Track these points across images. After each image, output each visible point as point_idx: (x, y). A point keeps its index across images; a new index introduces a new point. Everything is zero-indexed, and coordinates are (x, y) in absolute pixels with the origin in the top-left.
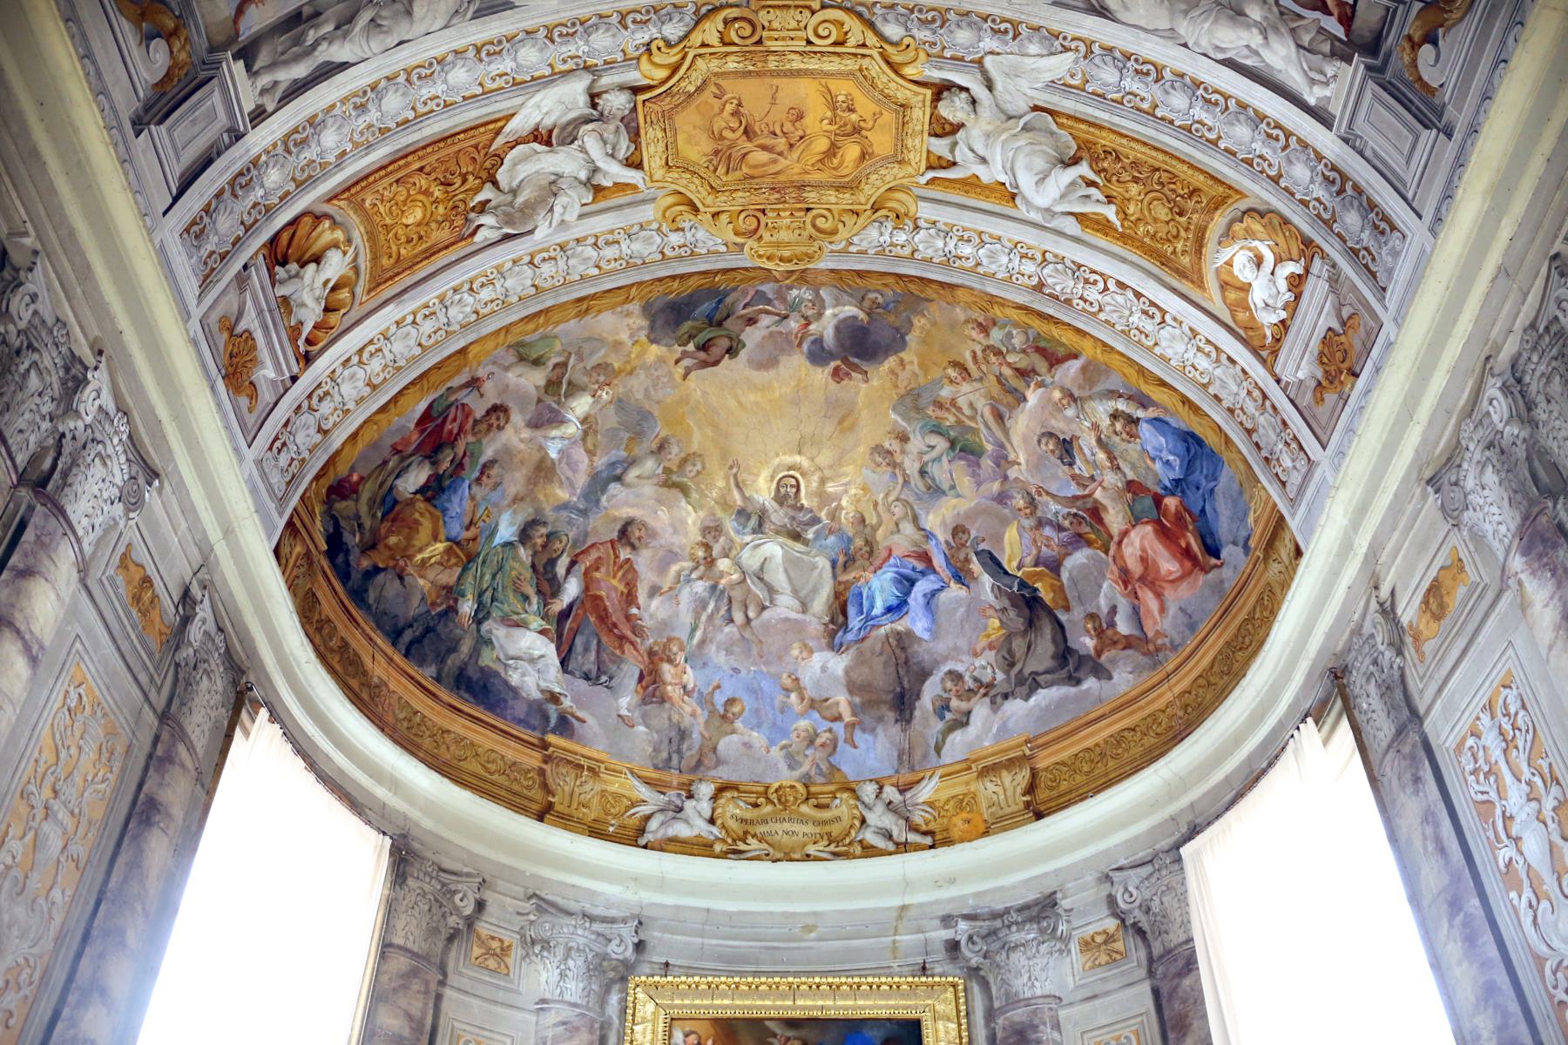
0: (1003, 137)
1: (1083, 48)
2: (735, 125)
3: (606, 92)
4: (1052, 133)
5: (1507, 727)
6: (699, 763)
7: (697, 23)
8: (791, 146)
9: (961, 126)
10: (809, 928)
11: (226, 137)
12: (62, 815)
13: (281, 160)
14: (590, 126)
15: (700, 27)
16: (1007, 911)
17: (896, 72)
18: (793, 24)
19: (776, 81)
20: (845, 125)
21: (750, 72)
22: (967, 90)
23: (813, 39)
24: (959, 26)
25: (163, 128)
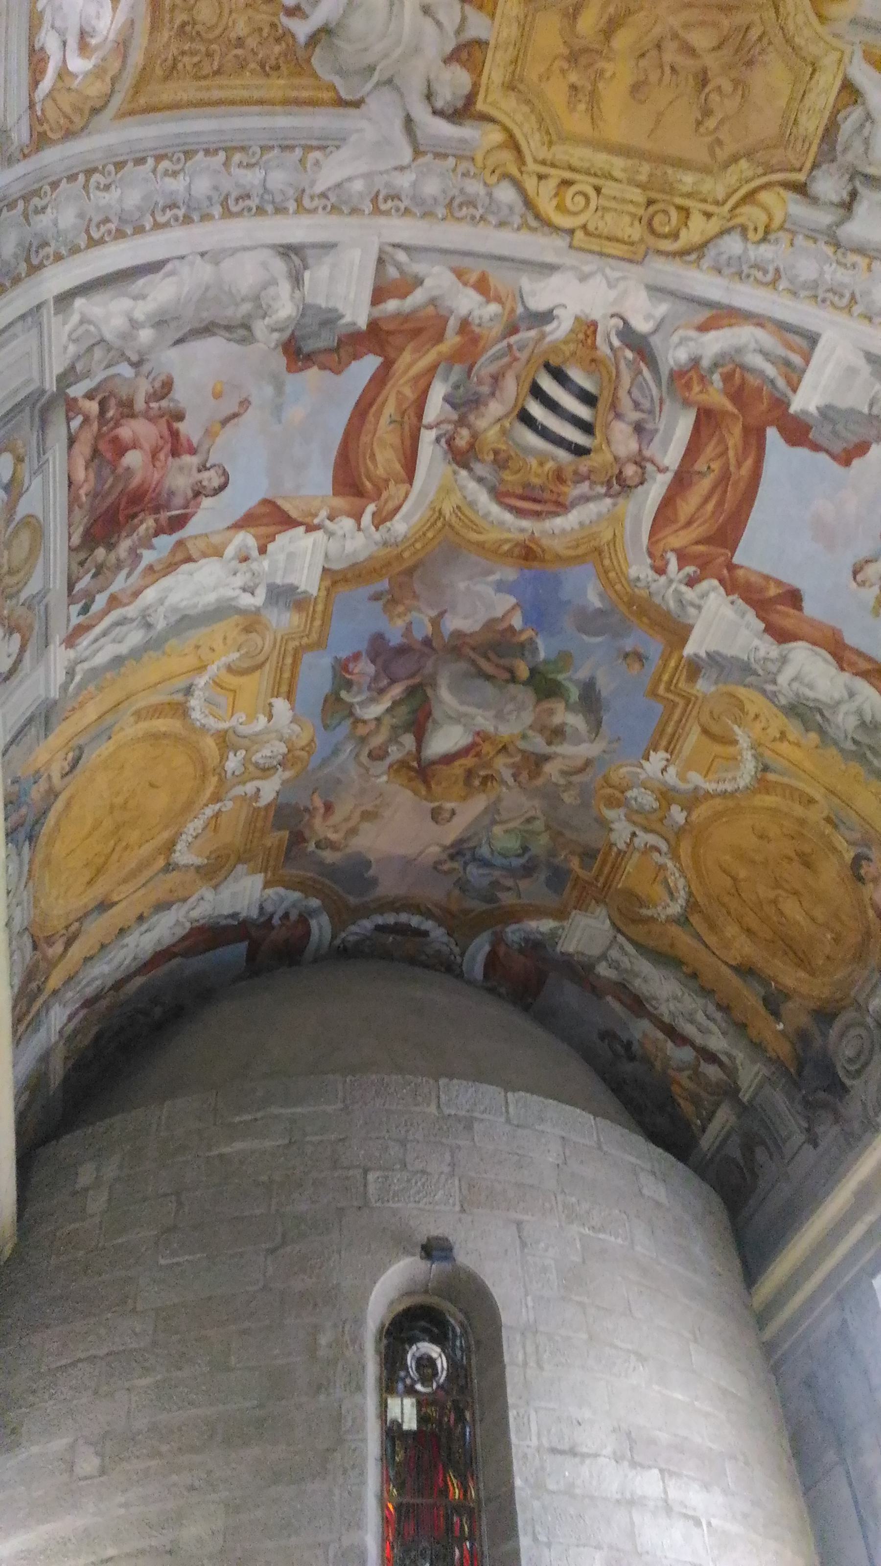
0: (399, 51)
1: (306, 202)
2: (715, 97)
3: (832, 204)
7: (705, 244)
8: (659, 47)
15: (704, 239)
17: (511, 136)
18: (609, 217)
19: (648, 145)
21: (673, 166)
22: (435, 112)
23: (592, 194)
24: (435, 200)
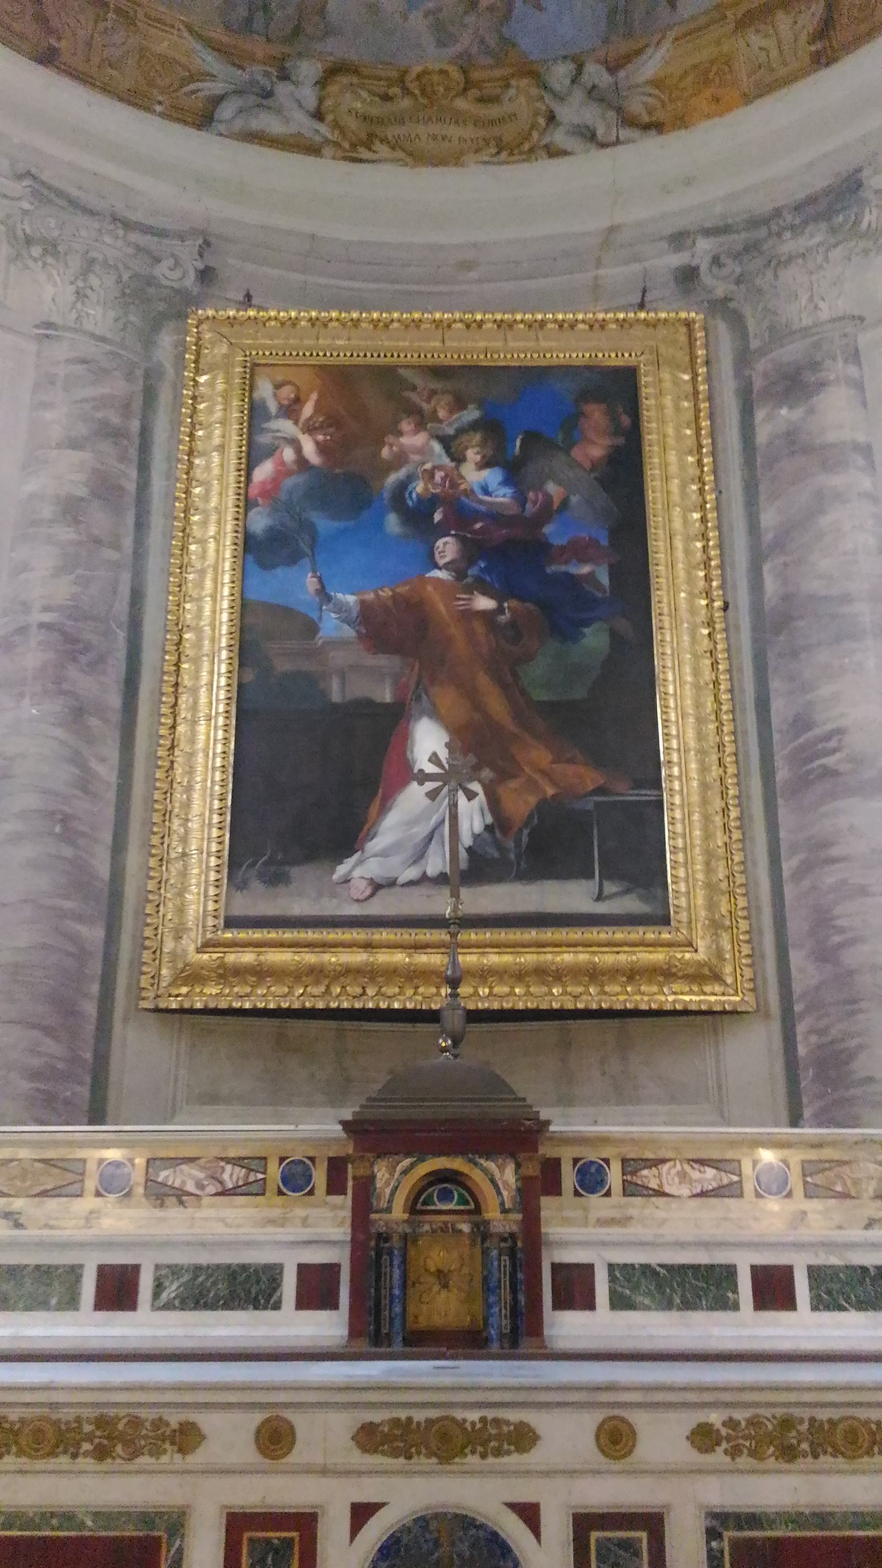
6: (297, 31)
10: (467, 266)
16: (777, 213)
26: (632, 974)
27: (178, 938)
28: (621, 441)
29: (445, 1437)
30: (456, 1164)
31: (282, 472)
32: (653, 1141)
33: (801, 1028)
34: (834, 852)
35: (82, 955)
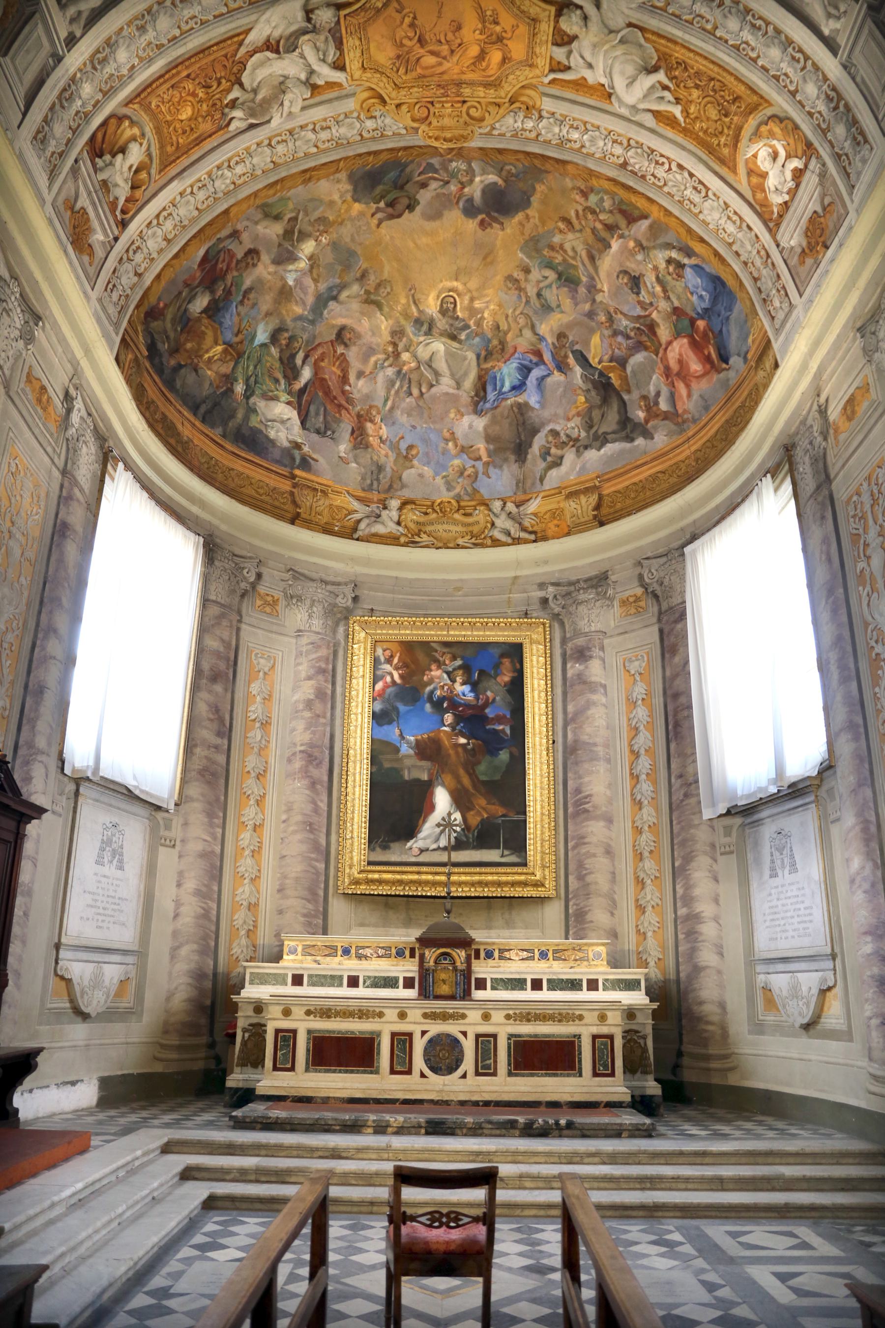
0: (605, 47)
2: (411, 34)
3: (317, 8)
4: (641, 46)
5: (876, 491)
8: (452, 52)
9: (575, 38)
10: (458, 589)
11: (50, 60)
12: (18, 536)
13: (91, 75)
14: (306, 37)
16: (578, 581)
20: (492, 35)
22: (581, 8)
25: (8, 59)
26: (513, 884)
27: (351, 868)
28: (516, 674)
29: (444, 1016)
30: (448, 950)
31: (386, 686)
32: (508, 944)
33: (571, 903)
34: (586, 840)
35: (317, 873)
